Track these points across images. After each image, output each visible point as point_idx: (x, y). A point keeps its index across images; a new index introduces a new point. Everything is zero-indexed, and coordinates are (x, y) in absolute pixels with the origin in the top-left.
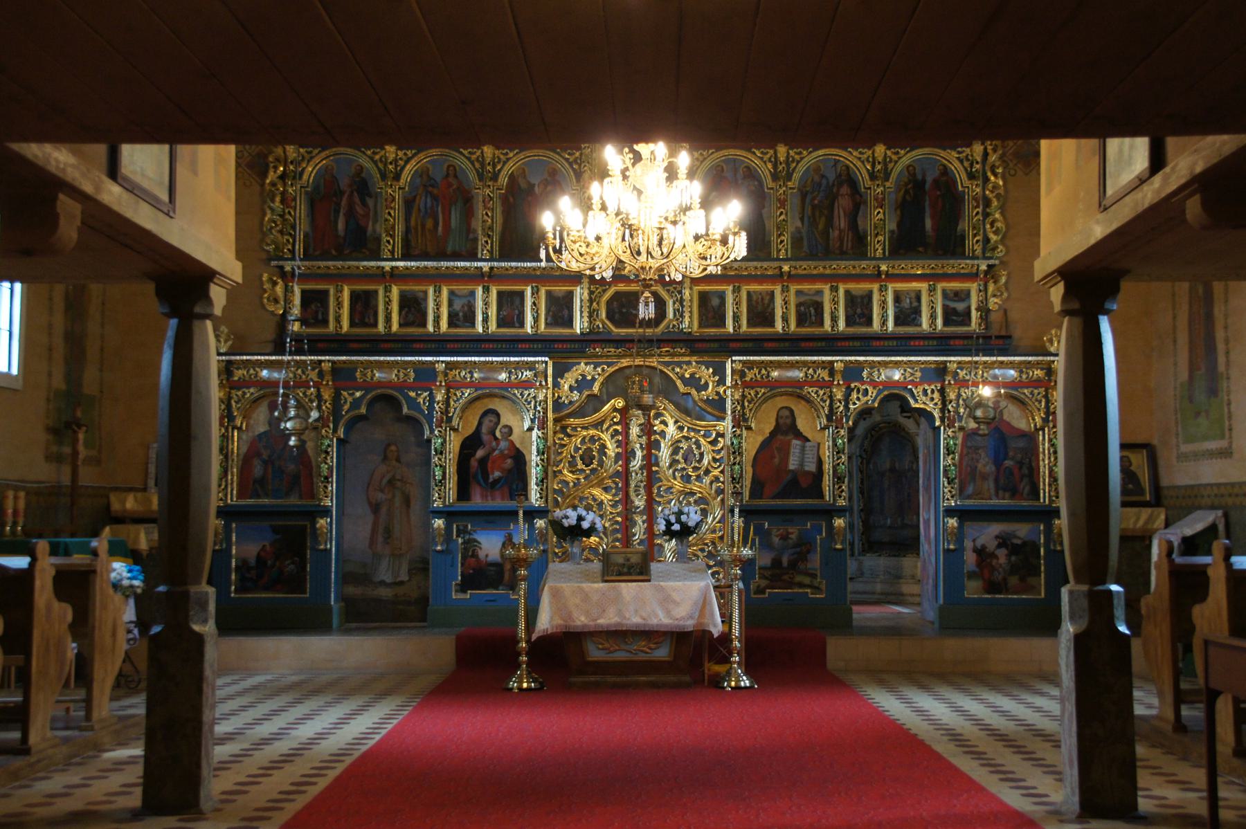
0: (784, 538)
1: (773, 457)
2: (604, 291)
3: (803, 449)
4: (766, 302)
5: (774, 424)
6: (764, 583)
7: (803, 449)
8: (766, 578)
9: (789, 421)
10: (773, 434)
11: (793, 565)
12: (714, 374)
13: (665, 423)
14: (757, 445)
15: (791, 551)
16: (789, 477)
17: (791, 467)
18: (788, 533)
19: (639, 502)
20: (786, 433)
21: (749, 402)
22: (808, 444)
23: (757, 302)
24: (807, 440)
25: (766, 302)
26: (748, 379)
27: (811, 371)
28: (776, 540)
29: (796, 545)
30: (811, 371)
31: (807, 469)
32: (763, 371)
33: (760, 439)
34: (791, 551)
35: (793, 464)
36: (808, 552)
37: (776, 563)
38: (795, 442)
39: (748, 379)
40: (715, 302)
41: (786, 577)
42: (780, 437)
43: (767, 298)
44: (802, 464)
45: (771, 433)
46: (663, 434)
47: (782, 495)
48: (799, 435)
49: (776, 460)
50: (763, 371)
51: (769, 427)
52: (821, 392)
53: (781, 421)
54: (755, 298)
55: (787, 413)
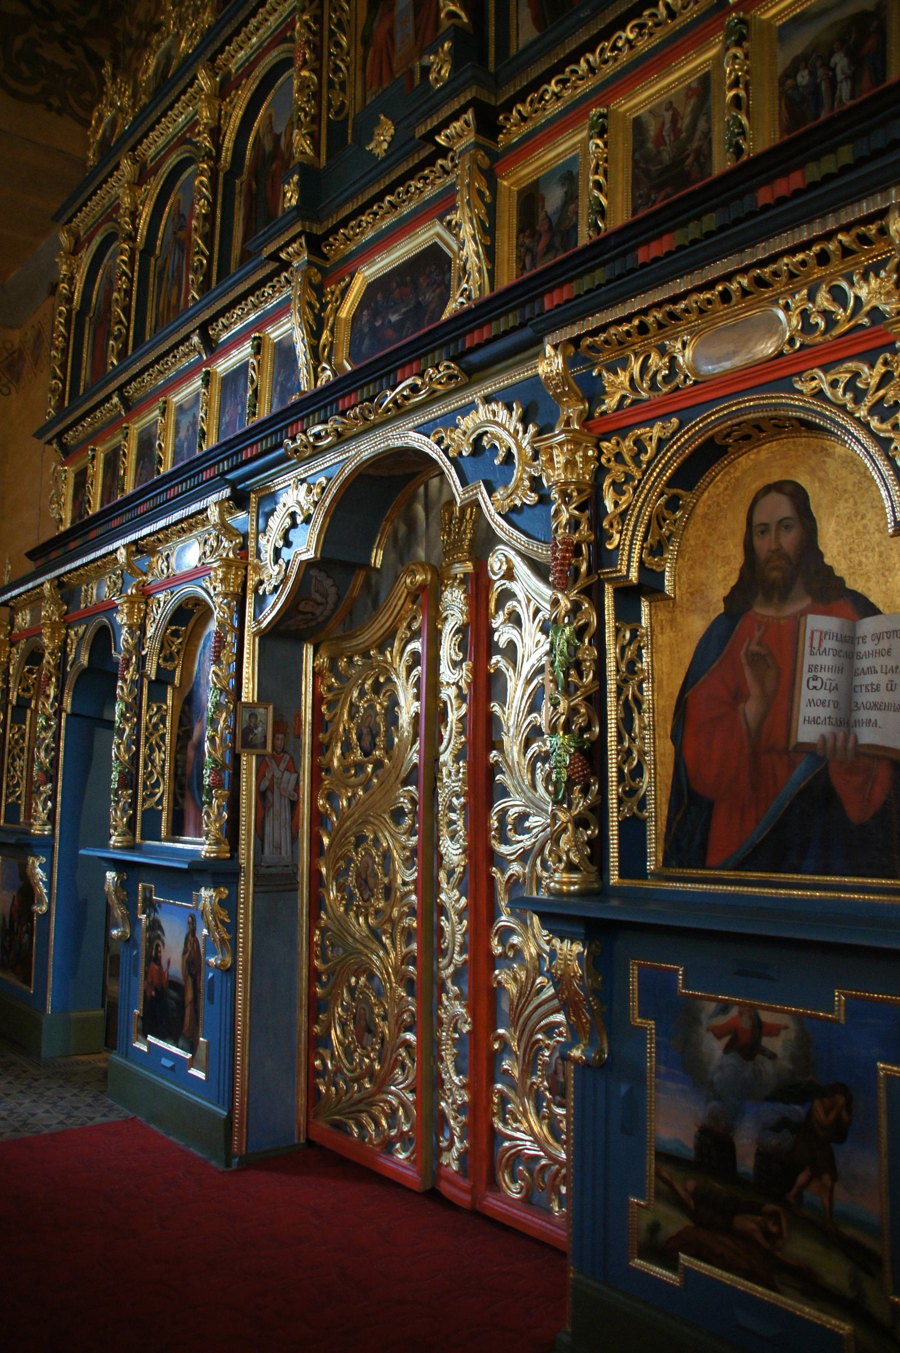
0: (746, 1044)
1: (739, 695)
2: (345, 291)
3: (849, 646)
4: (685, 123)
5: (738, 559)
6: (675, 1223)
7: (849, 646)
8: (676, 1201)
9: (789, 540)
10: (738, 601)
11: (777, 1172)
12: (525, 420)
13: (515, 620)
14: (688, 651)
15: (773, 1111)
16: (799, 776)
17: (807, 733)
18: (759, 1028)
19: (452, 851)
20: (780, 592)
21: (618, 488)
22: (868, 626)
23: (660, 140)
24: (867, 608)
25: (685, 123)
26: (611, 403)
27: (823, 299)
28: (714, 1048)
29: (789, 1091)
30: (823, 299)
31: (867, 736)
32: (655, 360)
33: (697, 626)
34: (773, 1111)
35: (811, 723)
36: (840, 1131)
37: (715, 1145)
38: (817, 623)
39: (611, 403)
40: (554, 199)
41: (747, 1223)
42: (762, 610)
43: (686, 111)
44: (845, 720)
45: (728, 600)
46: (511, 651)
47: (775, 852)
48: (832, 593)
49: (751, 709)
50: (655, 360)
51: (722, 578)
52: (871, 376)
53: (763, 545)
54: (652, 131)
55: (780, 507)
